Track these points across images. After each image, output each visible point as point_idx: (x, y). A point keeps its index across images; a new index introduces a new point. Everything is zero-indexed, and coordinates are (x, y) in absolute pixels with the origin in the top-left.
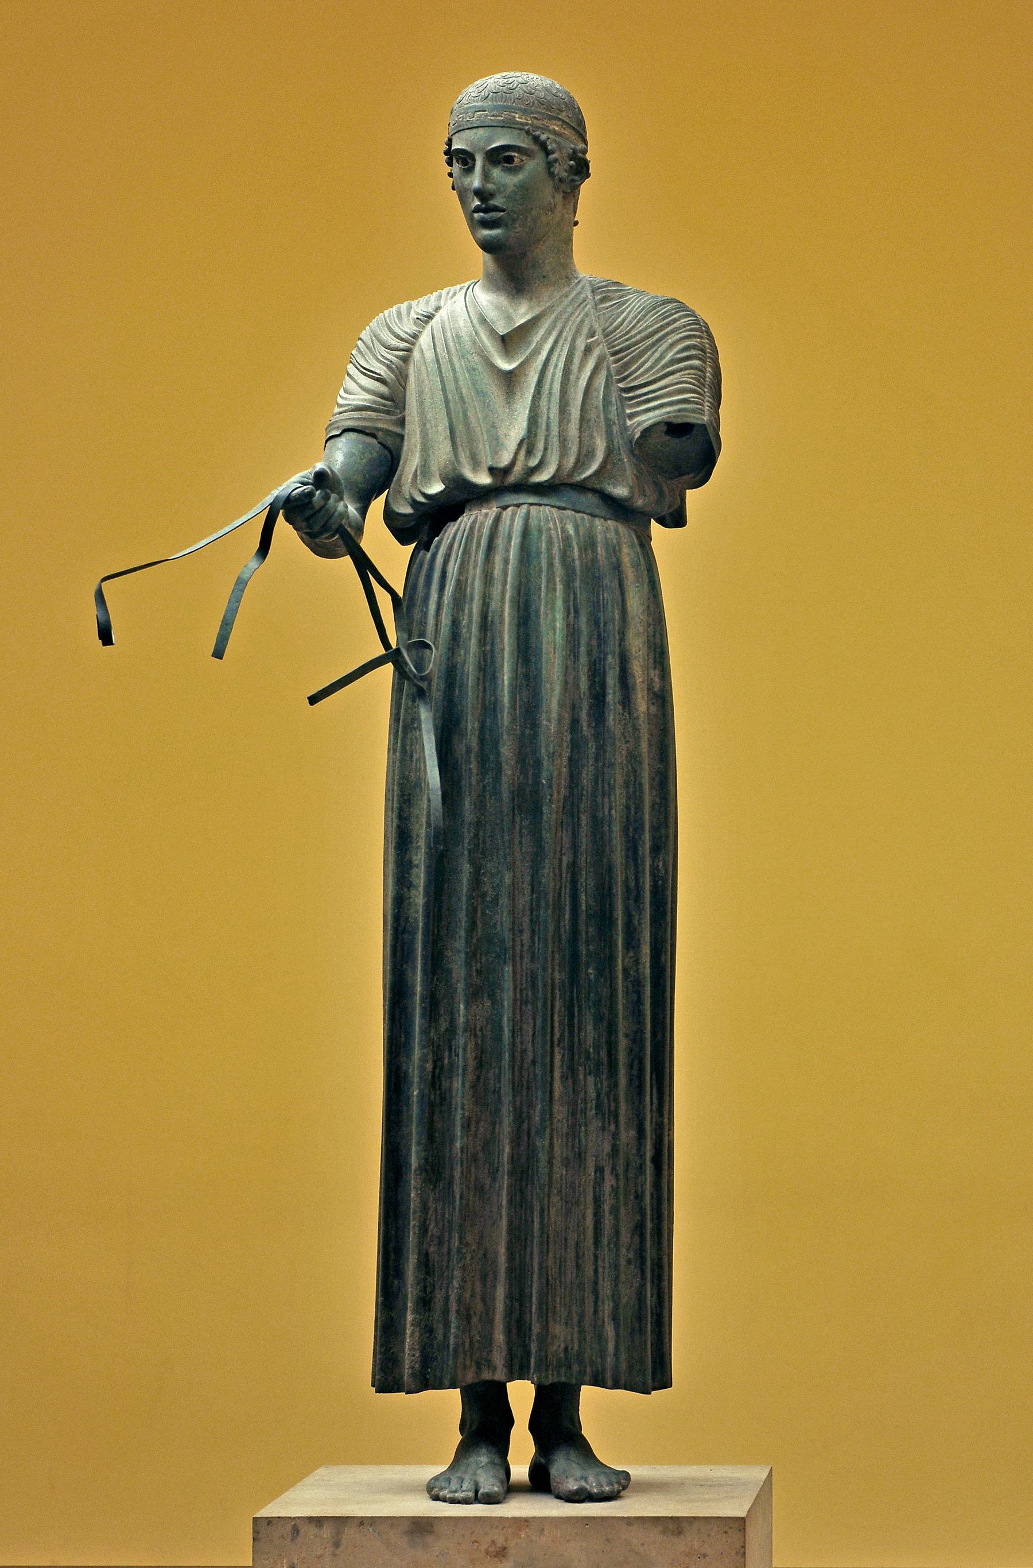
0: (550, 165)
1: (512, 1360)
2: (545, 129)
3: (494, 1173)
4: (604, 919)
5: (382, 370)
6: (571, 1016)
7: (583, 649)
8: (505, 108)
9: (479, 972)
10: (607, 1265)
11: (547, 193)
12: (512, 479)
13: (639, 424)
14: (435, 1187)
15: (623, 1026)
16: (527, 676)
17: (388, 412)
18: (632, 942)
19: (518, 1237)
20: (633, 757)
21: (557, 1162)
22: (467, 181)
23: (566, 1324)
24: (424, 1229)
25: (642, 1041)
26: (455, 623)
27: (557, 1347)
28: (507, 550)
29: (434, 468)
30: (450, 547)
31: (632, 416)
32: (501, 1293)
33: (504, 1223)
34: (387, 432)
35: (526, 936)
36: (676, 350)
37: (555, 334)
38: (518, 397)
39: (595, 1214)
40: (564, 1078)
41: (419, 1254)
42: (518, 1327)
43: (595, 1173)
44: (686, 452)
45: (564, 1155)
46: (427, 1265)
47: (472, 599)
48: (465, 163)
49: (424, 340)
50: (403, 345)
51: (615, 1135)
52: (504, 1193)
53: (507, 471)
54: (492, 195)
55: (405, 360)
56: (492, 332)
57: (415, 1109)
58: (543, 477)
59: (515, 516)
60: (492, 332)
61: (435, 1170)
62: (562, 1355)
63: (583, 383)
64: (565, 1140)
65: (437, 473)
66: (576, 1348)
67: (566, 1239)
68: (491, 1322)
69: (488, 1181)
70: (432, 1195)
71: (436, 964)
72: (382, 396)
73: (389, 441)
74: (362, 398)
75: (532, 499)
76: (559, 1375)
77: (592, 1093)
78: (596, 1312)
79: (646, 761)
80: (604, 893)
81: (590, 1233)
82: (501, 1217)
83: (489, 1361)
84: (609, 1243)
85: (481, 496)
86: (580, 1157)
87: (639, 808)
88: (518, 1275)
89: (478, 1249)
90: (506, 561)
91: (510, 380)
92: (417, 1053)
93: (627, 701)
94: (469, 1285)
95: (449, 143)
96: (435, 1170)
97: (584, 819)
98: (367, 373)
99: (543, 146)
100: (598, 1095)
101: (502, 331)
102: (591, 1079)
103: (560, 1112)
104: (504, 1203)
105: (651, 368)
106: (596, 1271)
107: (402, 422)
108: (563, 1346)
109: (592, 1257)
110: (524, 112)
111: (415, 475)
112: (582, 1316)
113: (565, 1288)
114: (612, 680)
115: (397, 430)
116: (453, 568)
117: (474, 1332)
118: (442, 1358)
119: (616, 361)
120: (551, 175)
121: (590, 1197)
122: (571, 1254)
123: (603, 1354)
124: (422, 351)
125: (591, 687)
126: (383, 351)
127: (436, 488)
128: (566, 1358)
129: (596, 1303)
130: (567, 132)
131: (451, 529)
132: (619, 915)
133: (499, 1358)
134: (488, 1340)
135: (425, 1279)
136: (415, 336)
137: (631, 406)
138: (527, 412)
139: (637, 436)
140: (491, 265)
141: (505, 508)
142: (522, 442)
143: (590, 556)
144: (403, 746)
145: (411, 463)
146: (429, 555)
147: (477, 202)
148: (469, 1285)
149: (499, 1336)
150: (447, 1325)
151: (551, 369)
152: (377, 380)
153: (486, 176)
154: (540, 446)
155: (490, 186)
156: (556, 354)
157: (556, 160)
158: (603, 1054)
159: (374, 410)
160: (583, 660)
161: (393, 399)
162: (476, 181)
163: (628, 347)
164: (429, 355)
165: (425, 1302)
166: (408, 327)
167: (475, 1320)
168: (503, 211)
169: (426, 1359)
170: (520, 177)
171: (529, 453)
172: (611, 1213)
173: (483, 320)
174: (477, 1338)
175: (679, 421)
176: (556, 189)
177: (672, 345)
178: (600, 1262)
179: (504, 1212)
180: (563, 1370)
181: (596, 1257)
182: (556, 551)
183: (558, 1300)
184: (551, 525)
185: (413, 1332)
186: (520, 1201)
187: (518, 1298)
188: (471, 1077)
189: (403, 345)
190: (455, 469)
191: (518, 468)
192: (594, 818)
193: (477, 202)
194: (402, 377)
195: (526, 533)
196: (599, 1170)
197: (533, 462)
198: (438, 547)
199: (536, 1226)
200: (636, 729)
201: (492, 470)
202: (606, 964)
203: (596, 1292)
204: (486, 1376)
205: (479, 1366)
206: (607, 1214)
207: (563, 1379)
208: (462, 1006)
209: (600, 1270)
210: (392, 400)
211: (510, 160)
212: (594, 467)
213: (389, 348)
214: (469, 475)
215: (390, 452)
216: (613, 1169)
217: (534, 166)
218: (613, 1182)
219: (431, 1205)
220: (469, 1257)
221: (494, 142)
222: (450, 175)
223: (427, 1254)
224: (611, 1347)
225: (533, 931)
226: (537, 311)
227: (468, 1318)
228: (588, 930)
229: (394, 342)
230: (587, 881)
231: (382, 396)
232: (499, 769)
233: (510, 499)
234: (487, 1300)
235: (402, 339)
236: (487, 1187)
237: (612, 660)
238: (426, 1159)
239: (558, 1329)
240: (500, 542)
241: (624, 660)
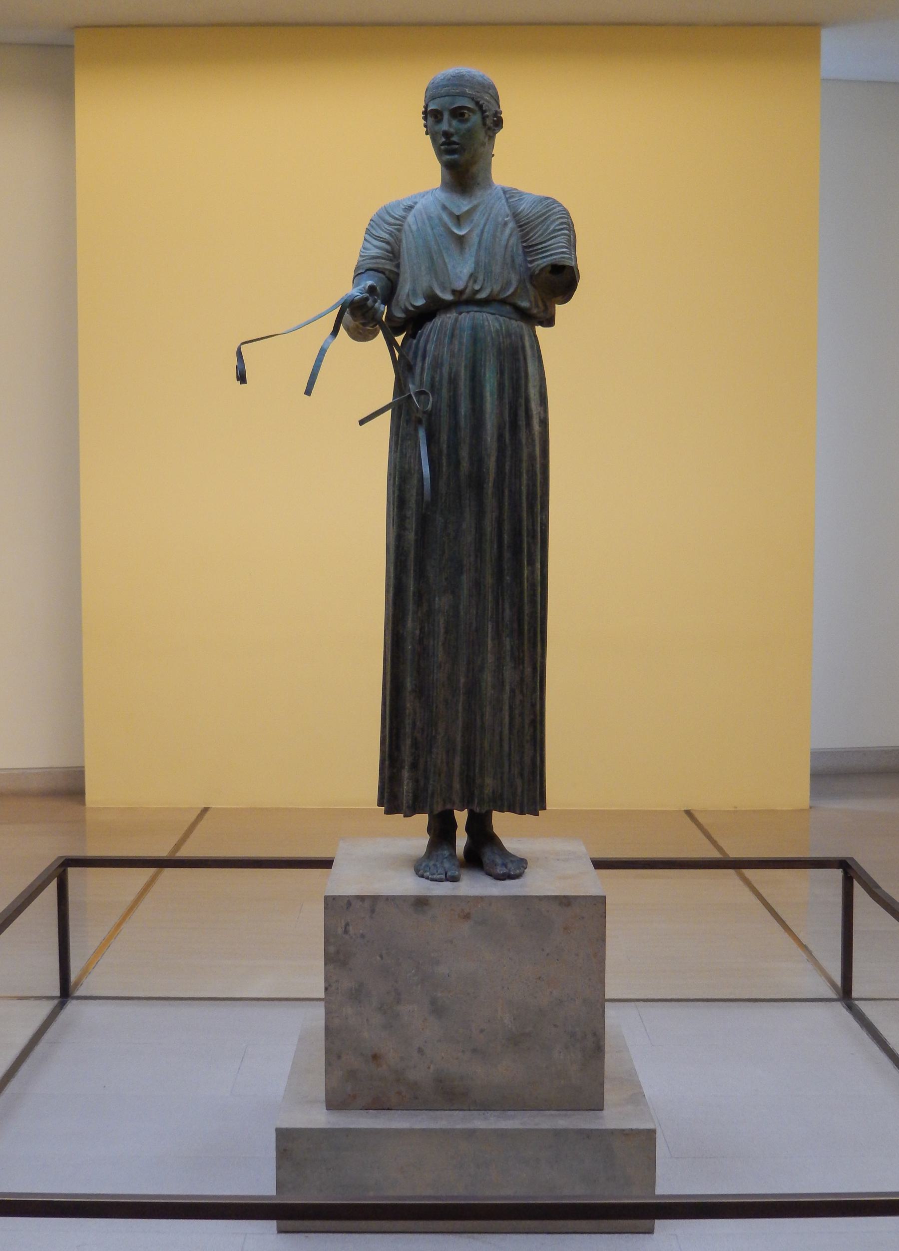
0: (484, 118)
2: (483, 98)
4: (517, 551)
5: (386, 236)
6: (497, 603)
7: (506, 395)
8: (461, 85)
9: (446, 579)
11: (481, 135)
12: (464, 297)
13: (538, 265)
15: (527, 609)
16: (473, 410)
17: (391, 260)
18: (531, 562)
20: (532, 458)
22: (437, 128)
24: (414, 723)
25: (536, 618)
26: (433, 378)
27: (488, 791)
28: (461, 337)
29: (419, 291)
30: (429, 336)
31: (531, 262)
32: (458, 761)
33: (460, 722)
34: (391, 271)
35: (472, 559)
36: (557, 223)
37: (486, 215)
38: (467, 250)
40: (493, 639)
44: (561, 281)
47: (442, 364)
48: (436, 117)
49: (410, 219)
50: (398, 222)
51: (523, 672)
52: (461, 704)
53: (462, 292)
54: (452, 135)
55: (399, 230)
56: (451, 214)
57: (409, 656)
58: (483, 295)
59: (466, 318)
60: (451, 214)
63: (503, 243)
65: (421, 295)
71: (421, 574)
72: (387, 251)
73: (392, 276)
74: (374, 252)
75: (476, 309)
77: (508, 647)
79: (538, 459)
80: (517, 534)
85: (446, 306)
86: (502, 683)
87: (534, 485)
88: (469, 752)
90: (461, 343)
91: (461, 241)
92: (409, 624)
93: (529, 425)
95: (426, 107)
96: (421, 691)
97: (506, 493)
98: (377, 238)
99: (480, 107)
100: (512, 647)
101: (458, 214)
102: (508, 639)
103: (490, 658)
104: (460, 708)
105: (542, 234)
106: (510, 748)
107: (398, 266)
110: (471, 88)
111: (408, 295)
112: (502, 773)
114: (522, 413)
115: (396, 270)
116: (431, 347)
119: (521, 231)
120: (484, 124)
122: (497, 738)
124: (409, 226)
125: (509, 416)
126: (387, 227)
127: (420, 302)
129: (510, 765)
130: (493, 101)
131: (429, 326)
132: (525, 546)
133: (456, 798)
134: (450, 787)
136: (405, 218)
137: (531, 256)
138: (473, 259)
139: (537, 272)
140: (448, 177)
141: (460, 313)
142: (471, 275)
143: (509, 341)
144: (401, 450)
145: (405, 288)
146: (415, 341)
147: (444, 140)
149: (457, 786)
150: (427, 778)
151: (485, 234)
152: (384, 242)
153: (450, 125)
154: (481, 277)
155: (452, 130)
156: (487, 227)
157: (488, 116)
158: (515, 626)
159: (383, 258)
160: (507, 401)
161: (394, 254)
162: (444, 126)
163: (528, 223)
164: (414, 227)
165: (414, 766)
166: (399, 212)
168: (458, 144)
169: (416, 798)
170: (469, 125)
171: (475, 282)
173: (444, 208)
175: (562, 263)
176: (486, 133)
177: (554, 221)
179: (460, 715)
181: (510, 739)
182: (489, 338)
184: (486, 323)
185: (408, 783)
187: (468, 763)
188: (442, 638)
189: (398, 222)
190: (433, 291)
191: (468, 291)
192: (510, 491)
193: (444, 140)
194: (399, 241)
195: (474, 328)
196: (513, 691)
197: (477, 287)
198: (420, 337)
200: (533, 440)
201: (454, 292)
202: (517, 575)
204: (449, 807)
208: (437, 599)
210: (392, 252)
211: (463, 115)
212: (511, 290)
213: (389, 224)
214: (439, 293)
215: (392, 282)
217: (476, 118)
221: (454, 104)
222: (425, 126)
223: (416, 739)
224: (519, 790)
225: (476, 556)
226: (475, 202)
227: (440, 775)
228: (507, 555)
229: (393, 221)
230: (507, 527)
231: (387, 251)
232: (458, 464)
233: (464, 308)
235: (397, 219)
237: (522, 401)
239: (489, 781)
240: (457, 332)
241: (527, 400)
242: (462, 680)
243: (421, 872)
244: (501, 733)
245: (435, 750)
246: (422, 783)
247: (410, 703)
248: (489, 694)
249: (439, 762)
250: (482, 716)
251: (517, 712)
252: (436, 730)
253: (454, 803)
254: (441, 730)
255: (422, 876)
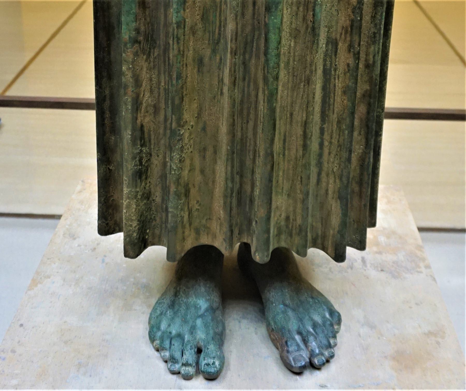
1: (232, 232)
3: (215, 44)
10: (335, 141)
14: (149, 55)
19: (242, 111)
21: (285, 34)
23: (288, 195)
24: (137, 104)
32: (221, 170)
33: (226, 101)
39: (324, 88)
41: (134, 130)
42: (239, 200)
43: (327, 44)
45: (294, 26)
46: (142, 138)
61: (148, 40)
62: (283, 223)
64: (295, 8)
66: (299, 221)
67: (291, 115)
68: (211, 193)
69: (208, 52)
70: (145, 65)
76: (278, 242)
78: (319, 181)
81: (317, 108)
82: (222, 93)
83: (208, 230)
84: (339, 122)
86: (314, 31)
88: (240, 151)
89: (197, 123)
94: (188, 162)
96: (148, 40)
106: (321, 145)
108: (283, 215)
109: (318, 131)
113: (289, 161)
117: (193, 203)
118: (161, 218)
121: (320, 72)
123: (325, 221)
128: (287, 226)
129: (319, 174)
134: (208, 212)
135: (141, 151)
148: (188, 162)
149: (219, 210)
167: (193, 191)
172: (344, 93)
174: (197, 207)
178: (326, 136)
180: (283, 237)
181: (322, 131)
183: (281, 174)
185: (128, 207)
186: (242, 76)
196: (333, 43)
199: (262, 107)
203: (320, 164)
204: (205, 240)
205: (198, 232)
206: (339, 92)
207: (283, 244)
209: (326, 143)
216: (351, 47)
218: (351, 61)
219: (144, 75)
220: (187, 135)
227: (187, 193)
234: (207, 175)
236: (206, 60)
238: (137, 30)
239: (280, 201)
242: (231, 26)
243: (157, 342)
244: (306, 124)
245: (176, 155)
246: (157, 197)
247: (129, 62)
248: (284, 50)
249: (185, 173)
250: (272, 96)
251: (339, 84)
252: (179, 119)
253: (214, 236)
254: (186, 116)
255: (158, 350)
